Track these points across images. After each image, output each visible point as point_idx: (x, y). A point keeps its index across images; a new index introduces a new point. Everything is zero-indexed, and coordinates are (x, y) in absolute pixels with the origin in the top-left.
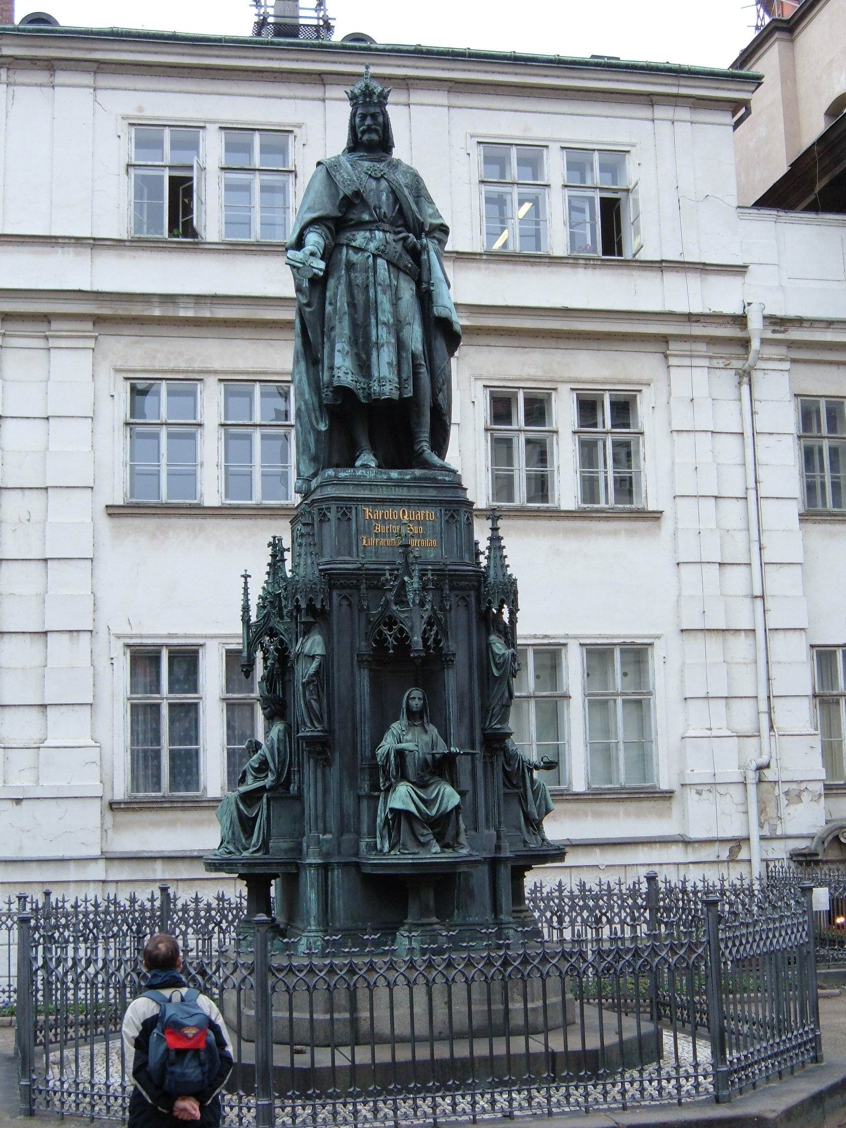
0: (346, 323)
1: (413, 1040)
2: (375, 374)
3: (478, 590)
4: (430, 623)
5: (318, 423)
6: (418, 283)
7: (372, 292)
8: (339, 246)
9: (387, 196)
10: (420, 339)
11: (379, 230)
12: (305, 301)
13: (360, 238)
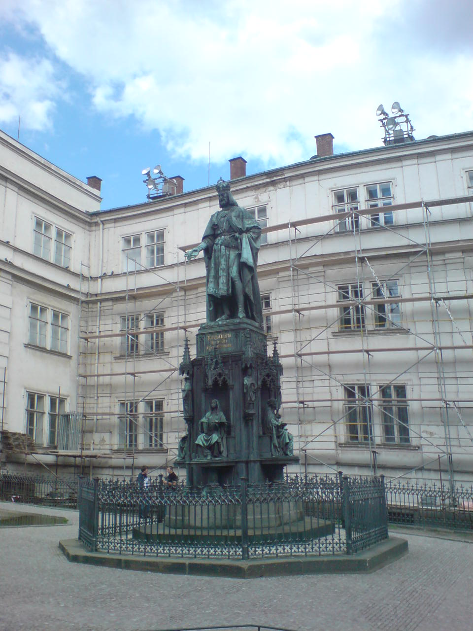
1: (202, 528)
4: (220, 375)
10: (235, 272)
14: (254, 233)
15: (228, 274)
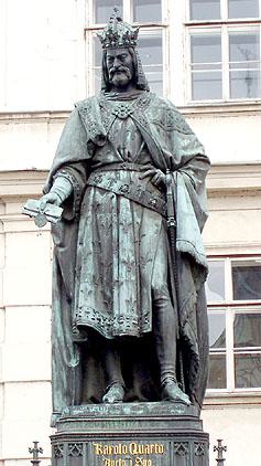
2: (116, 312)
5: (69, 360)
6: (166, 217)
7: (115, 231)
10: (161, 275)
12: (58, 242)
13: (105, 178)
14: (196, 171)
15: (141, 281)
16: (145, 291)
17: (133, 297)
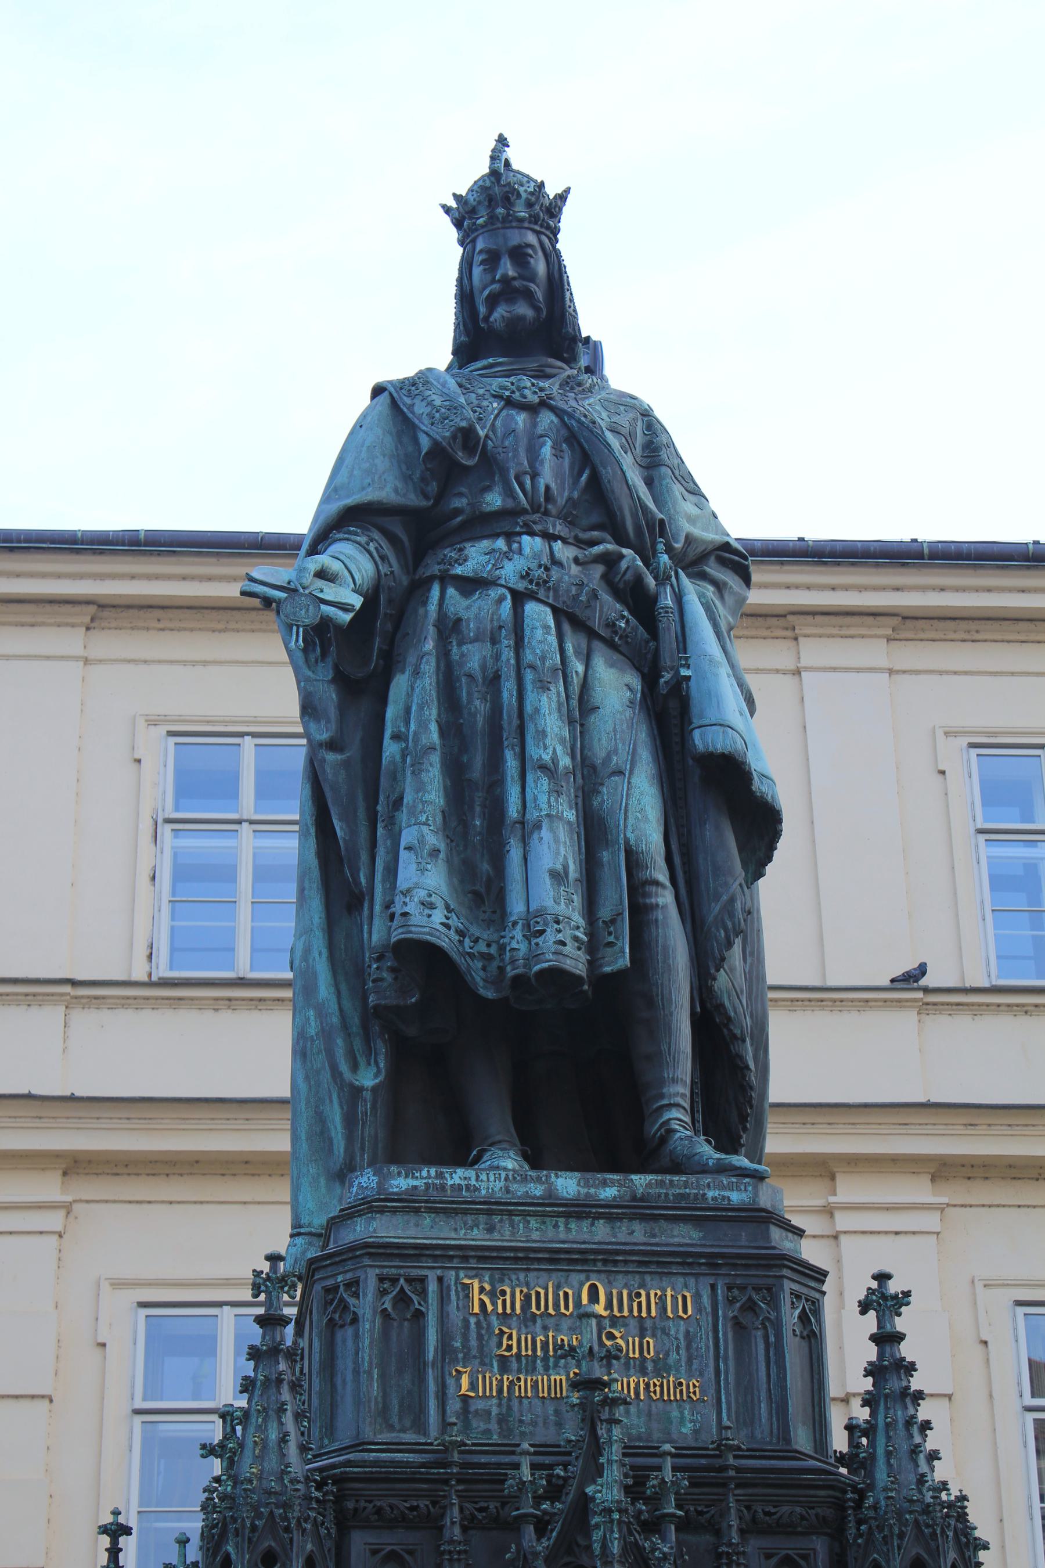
0: (434, 774)
2: (516, 907)
3: (837, 1533)
5: (355, 1067)
6: (650, 676)
7: (508, 687)
8: (418, 588)
9: (557, 454)
11: (532, 534)
12: (325, 736)
13: (475, 557)
16: (606, 856)
17: (572, 867)
